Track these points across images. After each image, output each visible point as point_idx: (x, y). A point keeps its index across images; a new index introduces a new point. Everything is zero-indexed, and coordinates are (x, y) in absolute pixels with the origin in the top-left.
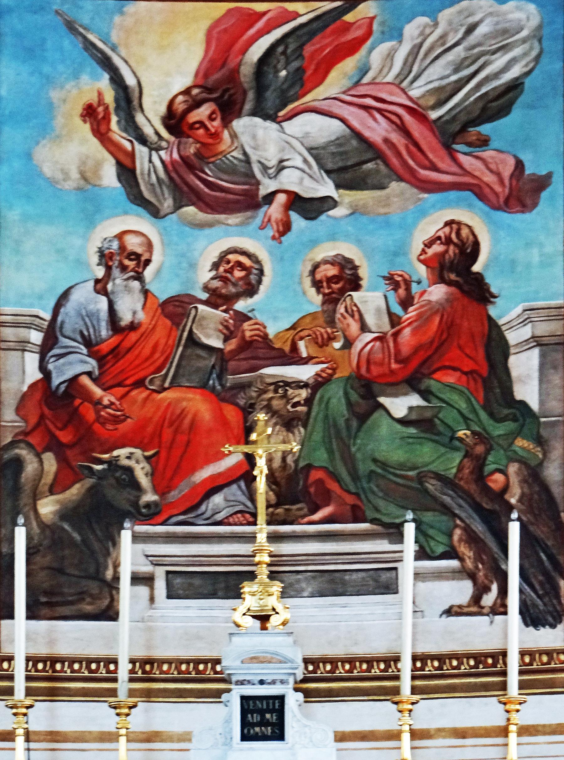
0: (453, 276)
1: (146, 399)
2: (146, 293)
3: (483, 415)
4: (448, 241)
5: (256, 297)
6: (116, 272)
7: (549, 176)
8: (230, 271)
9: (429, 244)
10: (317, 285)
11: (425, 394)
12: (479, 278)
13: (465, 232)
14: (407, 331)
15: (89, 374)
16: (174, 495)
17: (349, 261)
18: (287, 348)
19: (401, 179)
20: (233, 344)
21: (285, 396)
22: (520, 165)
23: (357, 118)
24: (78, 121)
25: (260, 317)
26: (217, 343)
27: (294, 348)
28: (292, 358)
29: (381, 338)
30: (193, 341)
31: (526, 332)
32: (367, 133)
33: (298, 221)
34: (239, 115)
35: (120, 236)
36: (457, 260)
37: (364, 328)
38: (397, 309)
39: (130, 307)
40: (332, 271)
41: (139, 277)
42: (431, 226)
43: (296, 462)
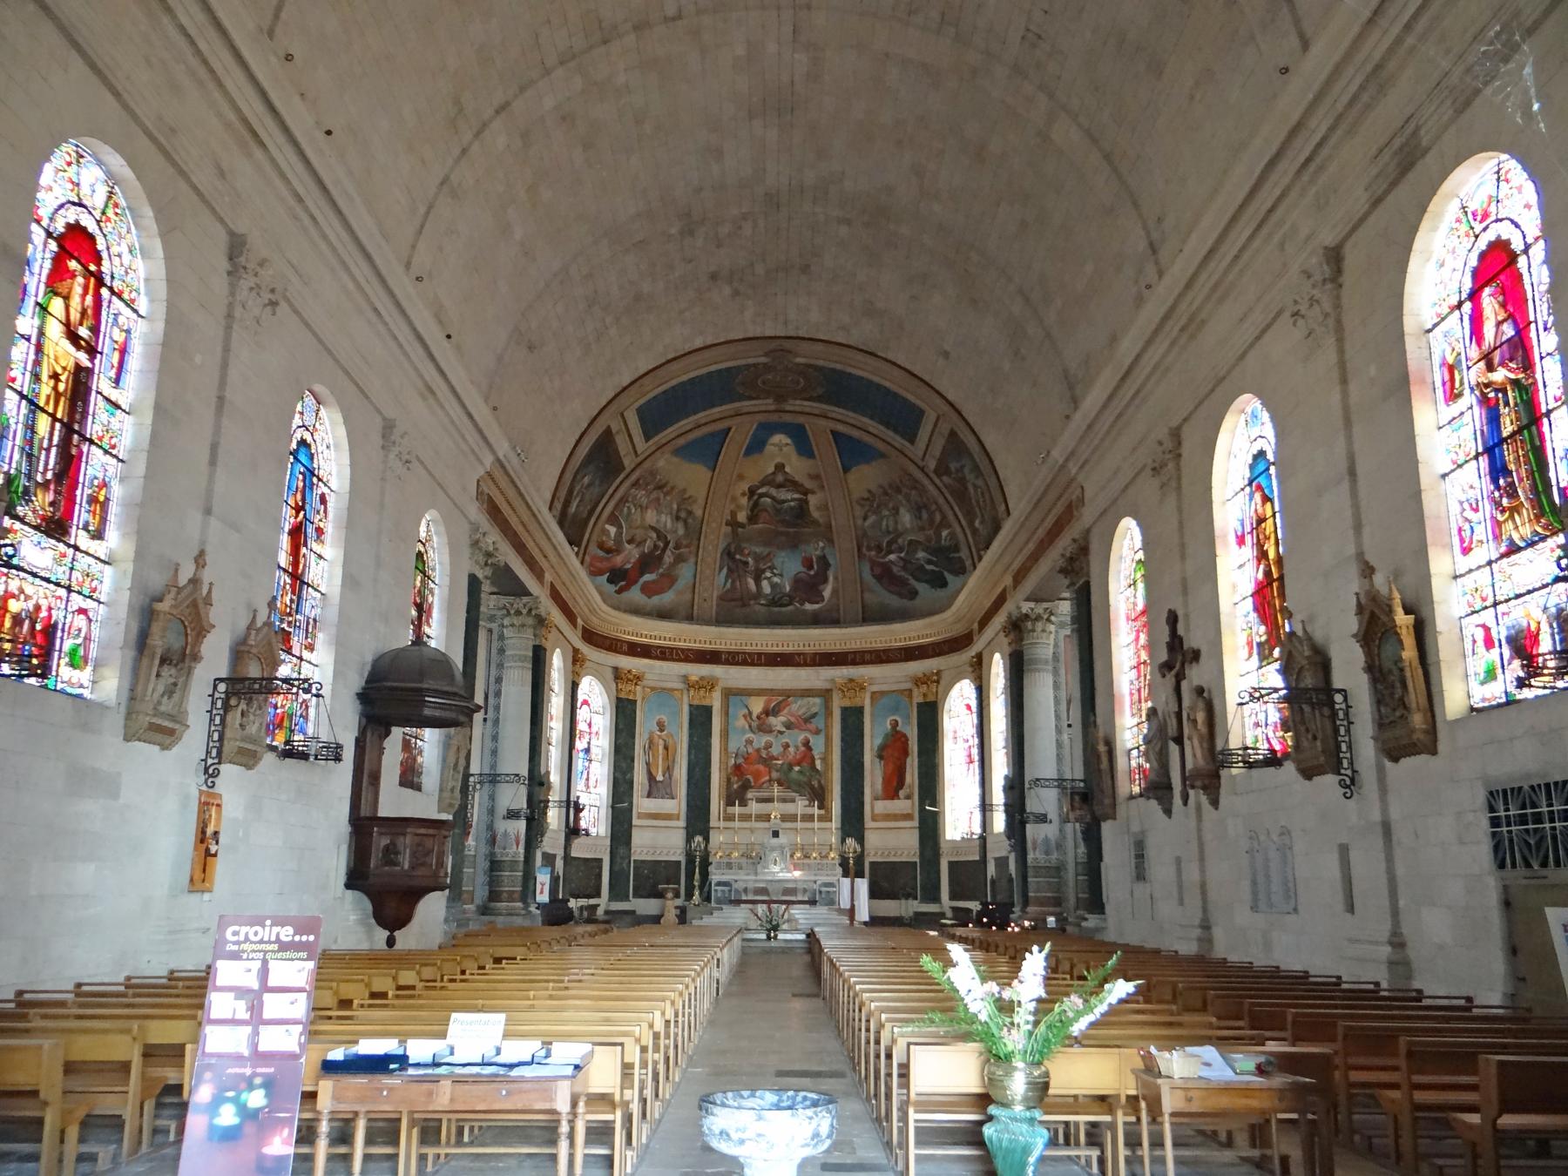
36: (807, 744)
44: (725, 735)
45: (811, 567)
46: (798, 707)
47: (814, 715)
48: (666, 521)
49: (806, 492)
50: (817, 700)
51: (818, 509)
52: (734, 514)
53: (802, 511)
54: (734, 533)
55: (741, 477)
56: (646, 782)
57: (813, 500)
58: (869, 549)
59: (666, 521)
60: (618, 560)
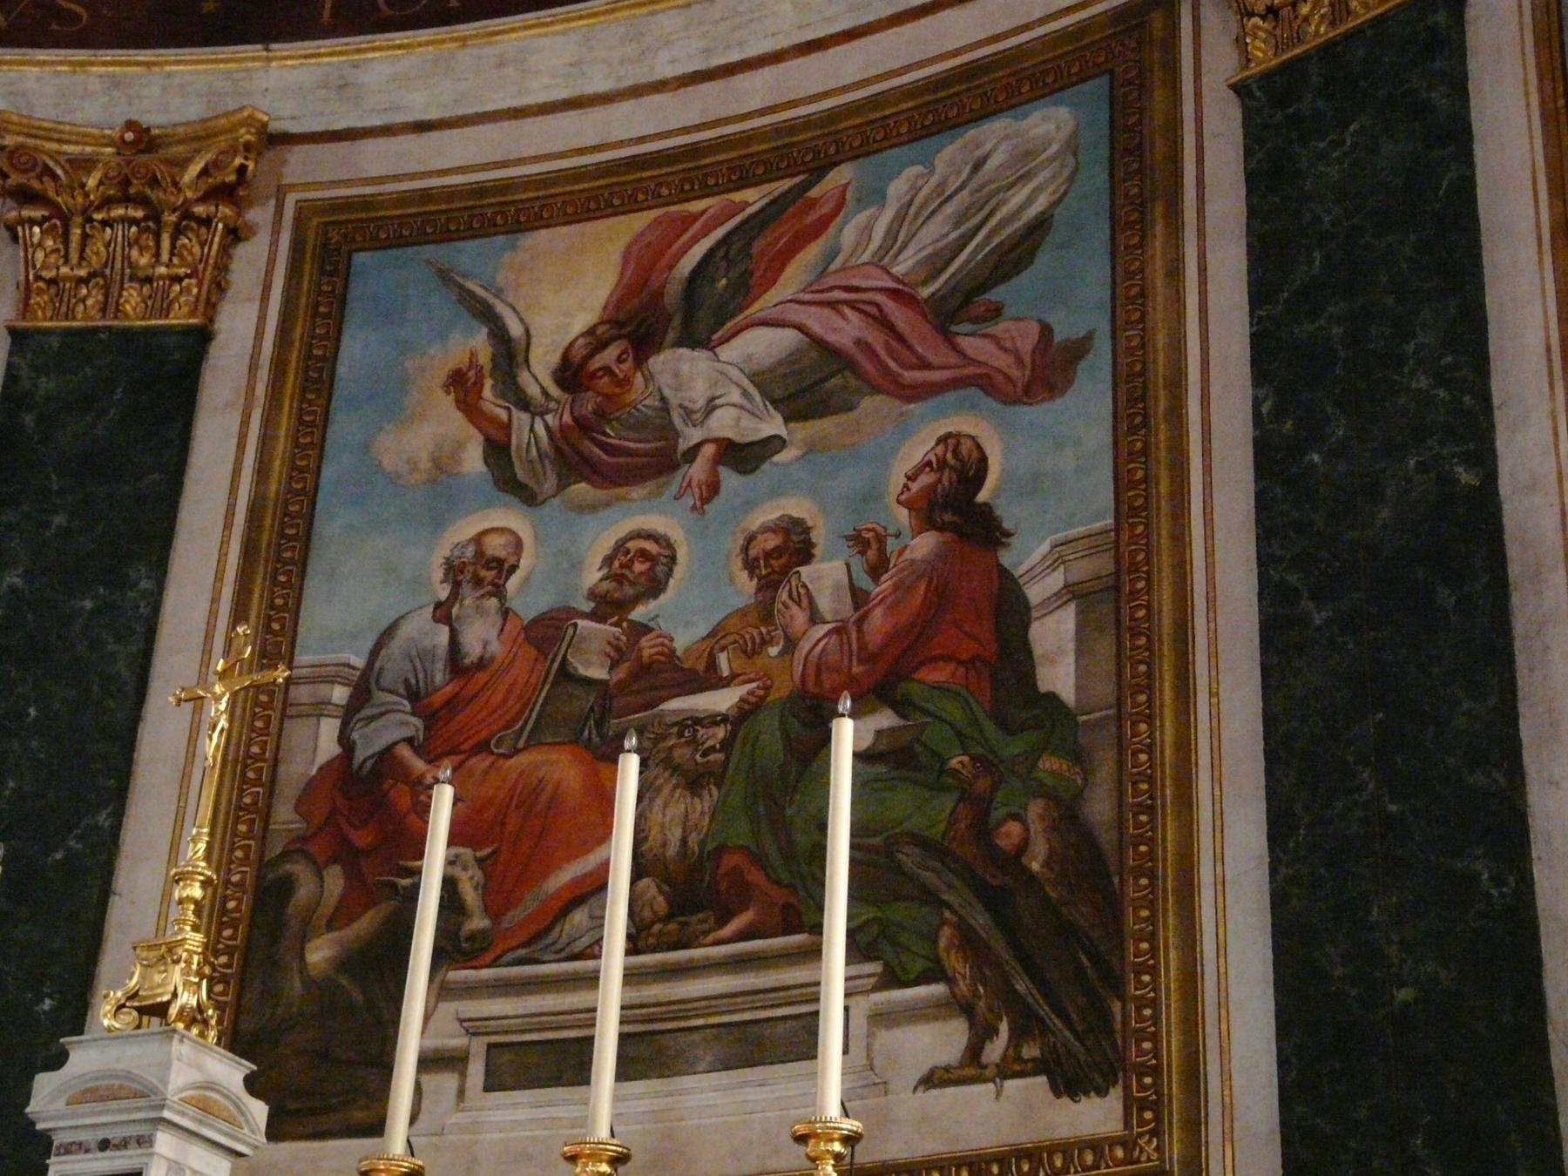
0: (948, 517)
1: (486, 772)
2: (505, 613)
3: (990, 727)
4: (942, 464)
5: (663, 598)
6: (466, 589)
7: (1089, 337)
8: (627, 566)
9: (911, 478)
10: (750, 565)
12: (986, 511)
13: (966, 446)
14: (877, 614)
15: (410, 741)
16: (515, 916)
18: (701, 667)
19: (877, 390)
20: (622, 672)
21: (694, 742)
22: (1046, 330)
23: (815, 320)
24: (440, 393)
25: (663, 625)
26: (598, 673)
27: (712, 664)
28: (710, 680)
30: (566, 674)
31: (1056, 580)
32: (831, 338)
33: (730, 479)
34: (659, 348)
35: (478, 539)
37: (815, 618)
38: (864, 581)
39: (481, 634)
40: (772, 541)
41: (498, 591)
42: (919, 448)
43: (702, 843)
46: (887, 223)
50: (1050, 122)
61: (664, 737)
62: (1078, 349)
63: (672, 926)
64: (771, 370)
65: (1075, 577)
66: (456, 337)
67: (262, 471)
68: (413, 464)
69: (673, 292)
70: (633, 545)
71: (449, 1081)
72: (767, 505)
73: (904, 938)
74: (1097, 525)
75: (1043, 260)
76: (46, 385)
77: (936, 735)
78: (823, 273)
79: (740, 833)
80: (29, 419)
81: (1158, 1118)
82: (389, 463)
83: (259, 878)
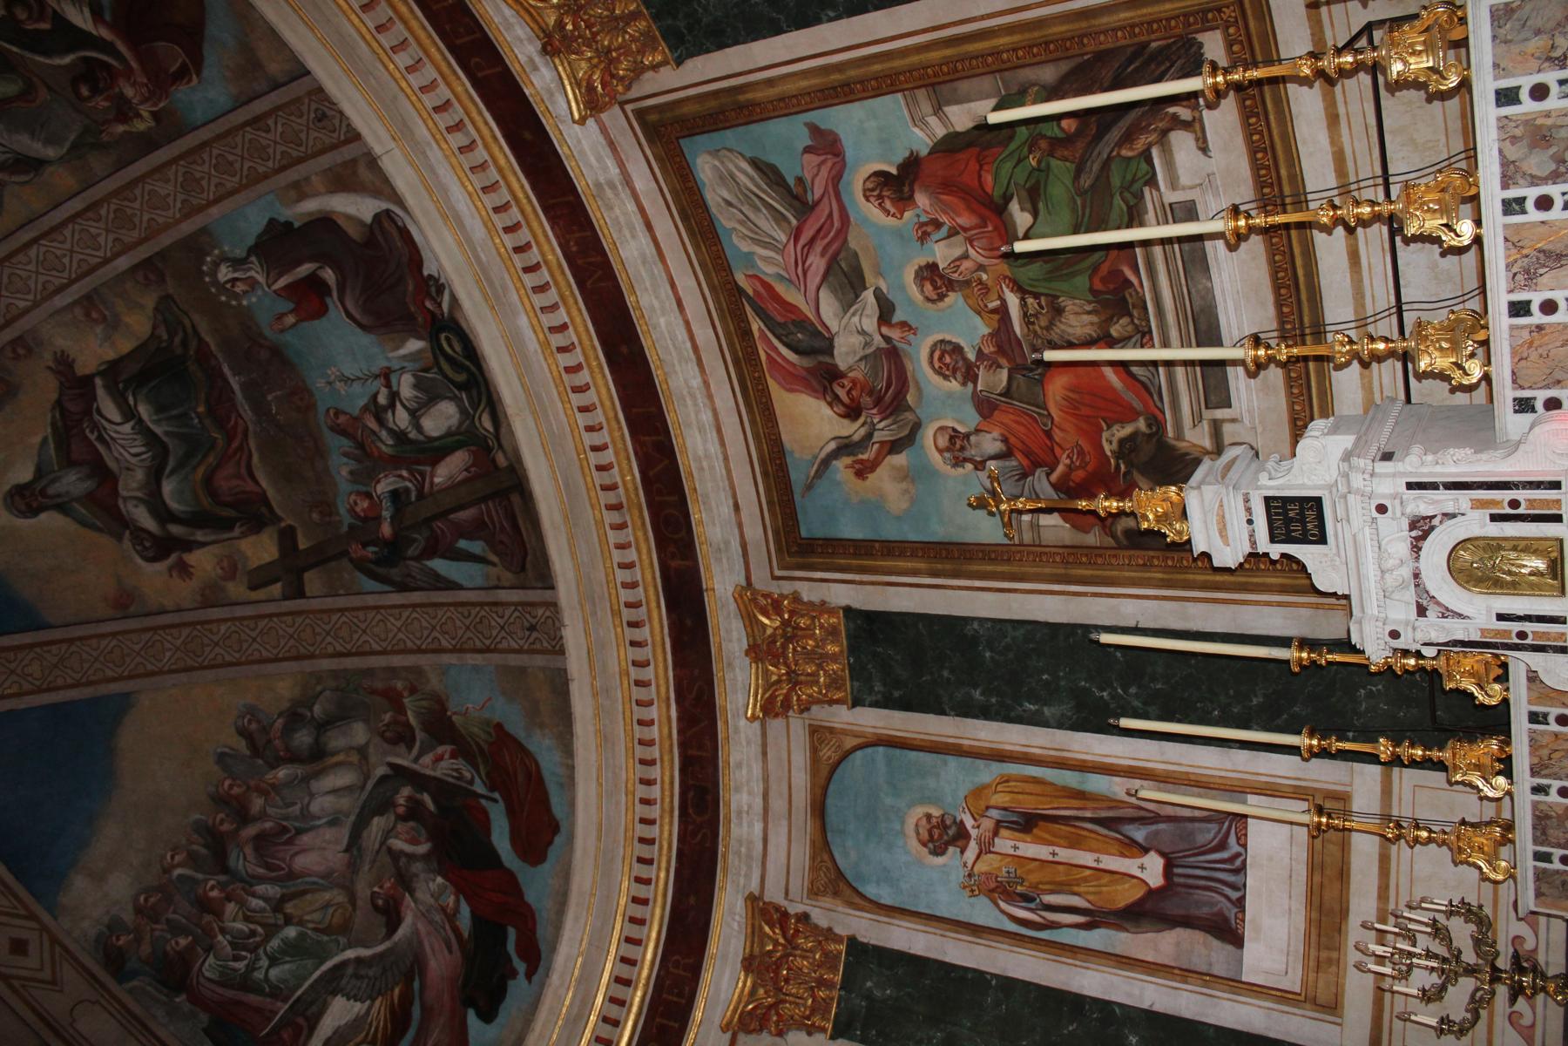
0: (906, 189)
1: (1062, 430)
2: (977, 431)
3: (1012, 146)
4: (880, 197)
5: (963, 344)
6: (967, 454)
7: (806, 124)
8: (947, 366)
9: (888, 213)
10: (941, 297)
11: (1007, 199)
12: (901, 167)
13: (870, 185)
14: (961, 221)
15: (1048, 475)
16: (1137, 404)
17: (917, 273)
18: (996, 317)
19: (845, 241)
20: (1003, 361)
21: (1035, 315)
22: (807, 150)
23: (814, 279)
24: (868, 483)
25: (977, 341)
26: (1004, 375)
27: (994, 311)
28: (1003, 311)
29: (970, 241)
30: (1007, 393)
31: (933, 121)
32: (822, 271)
33: (898, 316)
34: (836, 366)
35: (940, 451)
36: (894, 187)
37: (965, 256)
38: (944, 231)
39: (990, 443)
40: (928, 287)
41: (967, 436)
42: (872, 211)
43: (1089, 302)
44: (952, 558)
45: (314, 284)
46: (762, 249)
47: (768, 172)
48: (333, 791)
49: (76, 388)
50: (705, 168)
51: (113, 325)
52: (260, 578)
53: (157, 370)
54: (320, 557)
55: (124, 602)
56: (1164, 944)
57: (92, 351)
58: (124, 111)
59: (333, 791)
60: (441, 963)
61: (1035, 332)
62: (815, 130)
63: (1135, 313)
64: (840, 301)
65: (930, 110)
66: (838, 477)
67: (915, 573)
68: (906, 491)
69: (806, 362)
70: (937, 365)
71: (1227, 429)
72: (909, 293)
73: (1129, 177)
74: (902, 102)
75: (774, 159)
76: (878, 687)
77: (1020, 176)
78: (790, 281)
79: (1082, 281)
80: (896, 694)
81: (1210, 10)
82: (904, 505)
83: (1127, 548)
